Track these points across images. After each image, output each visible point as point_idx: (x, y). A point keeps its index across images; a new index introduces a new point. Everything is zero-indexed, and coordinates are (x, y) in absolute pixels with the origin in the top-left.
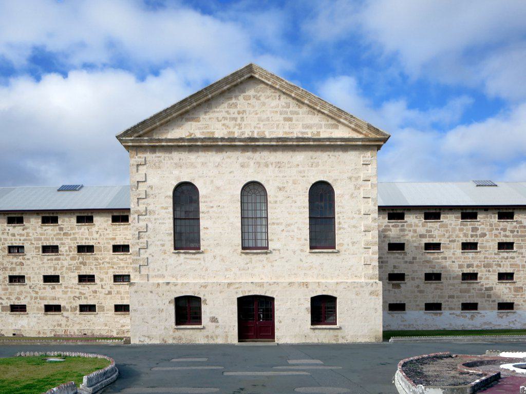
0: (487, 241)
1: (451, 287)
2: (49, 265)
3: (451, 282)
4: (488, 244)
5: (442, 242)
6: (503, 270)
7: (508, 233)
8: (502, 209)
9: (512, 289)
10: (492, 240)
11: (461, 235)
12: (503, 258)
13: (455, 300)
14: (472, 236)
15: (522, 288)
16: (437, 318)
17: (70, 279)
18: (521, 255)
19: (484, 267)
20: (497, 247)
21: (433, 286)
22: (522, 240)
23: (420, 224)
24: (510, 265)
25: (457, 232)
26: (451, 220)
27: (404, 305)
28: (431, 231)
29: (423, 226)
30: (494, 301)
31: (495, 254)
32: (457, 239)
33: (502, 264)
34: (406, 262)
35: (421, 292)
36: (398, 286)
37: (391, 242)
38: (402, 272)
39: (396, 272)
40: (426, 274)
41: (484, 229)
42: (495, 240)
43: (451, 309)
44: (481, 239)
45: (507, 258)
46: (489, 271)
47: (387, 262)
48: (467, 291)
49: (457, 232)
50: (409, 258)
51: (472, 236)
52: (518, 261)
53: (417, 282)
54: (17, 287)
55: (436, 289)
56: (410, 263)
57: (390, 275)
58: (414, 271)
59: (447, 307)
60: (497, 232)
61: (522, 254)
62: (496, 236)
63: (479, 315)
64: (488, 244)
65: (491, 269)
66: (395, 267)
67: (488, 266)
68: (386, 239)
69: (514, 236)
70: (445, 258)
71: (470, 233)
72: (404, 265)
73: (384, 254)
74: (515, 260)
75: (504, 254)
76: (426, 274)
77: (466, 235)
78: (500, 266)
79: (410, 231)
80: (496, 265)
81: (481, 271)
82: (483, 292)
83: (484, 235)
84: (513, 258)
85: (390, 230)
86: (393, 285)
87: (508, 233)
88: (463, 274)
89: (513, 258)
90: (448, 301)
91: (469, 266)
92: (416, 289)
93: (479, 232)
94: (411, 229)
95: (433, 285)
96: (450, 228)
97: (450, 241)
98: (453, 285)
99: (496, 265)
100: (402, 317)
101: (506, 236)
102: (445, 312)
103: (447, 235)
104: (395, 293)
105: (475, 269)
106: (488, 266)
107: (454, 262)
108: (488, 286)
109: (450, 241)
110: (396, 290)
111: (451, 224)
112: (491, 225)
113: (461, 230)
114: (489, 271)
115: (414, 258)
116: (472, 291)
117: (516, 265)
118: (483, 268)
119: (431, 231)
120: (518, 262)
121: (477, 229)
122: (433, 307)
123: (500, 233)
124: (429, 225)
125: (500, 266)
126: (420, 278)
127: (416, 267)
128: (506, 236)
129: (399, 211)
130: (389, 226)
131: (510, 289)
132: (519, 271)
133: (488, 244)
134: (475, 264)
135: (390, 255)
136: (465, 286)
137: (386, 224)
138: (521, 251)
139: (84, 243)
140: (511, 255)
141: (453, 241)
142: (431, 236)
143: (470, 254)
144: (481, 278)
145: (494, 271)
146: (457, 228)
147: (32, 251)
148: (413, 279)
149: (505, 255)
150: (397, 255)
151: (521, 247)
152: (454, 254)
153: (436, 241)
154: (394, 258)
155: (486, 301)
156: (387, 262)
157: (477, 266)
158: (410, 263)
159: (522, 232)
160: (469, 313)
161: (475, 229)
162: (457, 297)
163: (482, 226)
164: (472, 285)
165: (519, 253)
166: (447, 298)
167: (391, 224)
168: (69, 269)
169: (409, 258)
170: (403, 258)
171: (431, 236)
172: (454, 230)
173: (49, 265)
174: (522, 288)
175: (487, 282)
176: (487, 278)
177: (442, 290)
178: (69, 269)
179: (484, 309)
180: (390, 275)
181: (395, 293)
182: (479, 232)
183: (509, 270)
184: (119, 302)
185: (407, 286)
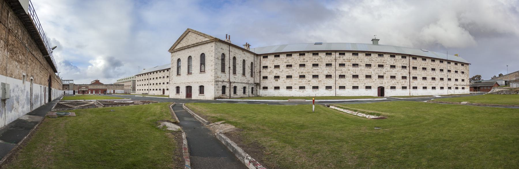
0: (308, 63)
1: (295, 81)
3: (296, 78)
4: (309, 64)
5: (292, 64)
6: (314, 74)
7: (316, 60)
8: (314, 52)
9: (318, 81)
10: (310, 63)
11: (299, 62)
12: (314, 69)
13: (297, 85)
14: (303, 62)
15: (321, 81)
16: (290, 92)
18: (321, 69)
19: (307, 73)
20: (312, 66)
21: (289, 80)
22: (321, 63)
23: (285, 58)
24: (317, 72)
25: (298, 60)
26: (295, 56)
27: (279, 87)
28: (288, 61)
29: (286, 59)
30: (311, 86)
31: (311, 68)
32: (298, 63)
33: (314, 72)
34: (280, 72)
35: (285, 82)
36: (277, 80)
37: (275, 65)
38: (279, 75)
39: (277, 75)
40: (287, 76)
41: (307, 59)
42: (311, 63)
43: (295, 89)
44: (306, 63)
45: (316, 70)
46: (309, 74)
47: (274, 72)
48: (301, 82)
49: (298, 60)
50: (281, 70)
51: (303, 62)
52: (320, 71)
53: (284, 79)
55: (290, 81)
56: (281, 72)
57: (275, 76)
58: (282, 75)
59: (294, 88)
60: (312, 60)
61: (321, 68)
62: (312, 61)
63: (305, 91)
64: (309, 65)
65: (310, 74)
66: (276, 74)
68: (273, 64)
69: (318, 62)
70: (293, 70)
71: (302, 61)
72: (280, 73)
73: (272, 69)
74: (319, 70)
75: (315, 68)
76: (287, 76)
77: (301, 61)
78: (313, 72)
79: (281, 61)
80: (311, 72)
81: (306, 75)
82: (307, 82)
83: (307, 61)
84: (318, 69)
85: (275, 61)
86: (276, 80)
87: (316, 60)
88: (300, 76)
89: (318, 69)
90: (294, 86)
91: (302, 73)
92: (283, 81)
93: (305, 60)
94: (282, 60)
95: (289, 80)
96: (295, 59)
97: (295, 64)
98: (296, 80)
99: (311, 72)
100: (279, 92)
101: (315, 62)
102: (293, 90)
103: (294, 62)
104: (276, 83)
105: (304, 74)
107: (296, 71)
108: (308, 80)
109: (295, 64)
110: (277, 82)
111: (295, 58)
112: (310, 58)
113: (299, 60)
114: (309, 74)
115: (283, 70)
116: (303, 82)
117: (319, 72)
118: (307, 73)
119: (288, 61)
120: (320, 71)
121: (305, 59)
123: (313, 60)
124: (288, 58)
125: (313, 72)
126: (285, 78)
127: (283, 73)
128: (315, 62)
129: (278, 54)
130: (274, 60)
131: (317, 81)
132: (320, 74)
133: (309, 64)
134: (304, 72)
135: (274, 70)
136: (300, 80)
137: (274, 59)
138: (321, 67)
140: (317, 68)
141: (296, 64)
142: (288, 62)
143: (302, 68)
144: (306, 77)
145: (311, 74)
146: (298, 59)
148: (282, 78)
149: (315, 68)
150: (277, 69)
151: (321, 66)
152: (296, 68)
153: (290, 64)
154: (276, 71)
155: (308, 85)
156: (274, 72)
157: (305, 73)
158: (281, 72)
159: (321, 60)
160: (302, 90)
161: (304, 59)
162: (298, 84)
163: (306, 58)
164: (303, 80)
165: (320, 68)
166: (294, 85)
167: (275, 59)
170: (279, 70)
171: (288, 62)
172: (296, 60)
174: (321, 81)
175: (308, 78)
176: (309, 77)
177: (292, 81)
179: (307, 89)
180: (275, 76)
181: (276, 83)
182: (305, 60)
183: (317, 74)
185: (280, 80)
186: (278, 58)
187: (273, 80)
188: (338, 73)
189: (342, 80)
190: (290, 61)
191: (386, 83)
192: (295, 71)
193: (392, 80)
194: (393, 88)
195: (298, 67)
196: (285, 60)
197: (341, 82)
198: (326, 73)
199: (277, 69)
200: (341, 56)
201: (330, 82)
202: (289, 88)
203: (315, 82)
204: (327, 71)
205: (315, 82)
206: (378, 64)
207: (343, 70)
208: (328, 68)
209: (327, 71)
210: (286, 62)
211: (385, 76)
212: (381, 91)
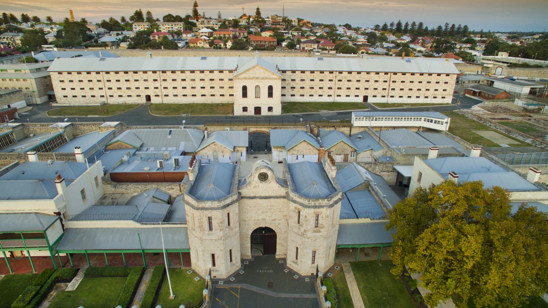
2: (202, 84)
17: (208, 88)
48: (311, 92)
52: (324, 84)
54: (194, 90)
67: (316, 85)
83: (316, 77)
106: (316, 85)
122: (302, 95)
139: (211, 78)
143: (312, 82)
147: (197, 80)
161: (314, 76)
168: (208, 85)
169: (296, 83)
173: (202, 84)
178: (208, 85)
184: (221, 94)
186: (294, 74)
187: (290, 90)
188: (337, 86)
189: (339, 90)
190: (303, 77)
191: (370, 93)
192: (306, 84)
193: (374, 90)
194: (374, 96)
195: (309, 81)
196: (300, 76)
197: (339, 92)
198: (329, 86)
199: (293, 82)
200: (340, 74)
201: (331, 92)
202: (302, 95)
203: (320, 92)
204: (330, 84)
205: (320, 92)
206: (365, 80)
207: (340, 84)
208: (330, 82)
209: (330, 84)
210: (300, 77)
211: (369, 88)
212: (366, 98)
